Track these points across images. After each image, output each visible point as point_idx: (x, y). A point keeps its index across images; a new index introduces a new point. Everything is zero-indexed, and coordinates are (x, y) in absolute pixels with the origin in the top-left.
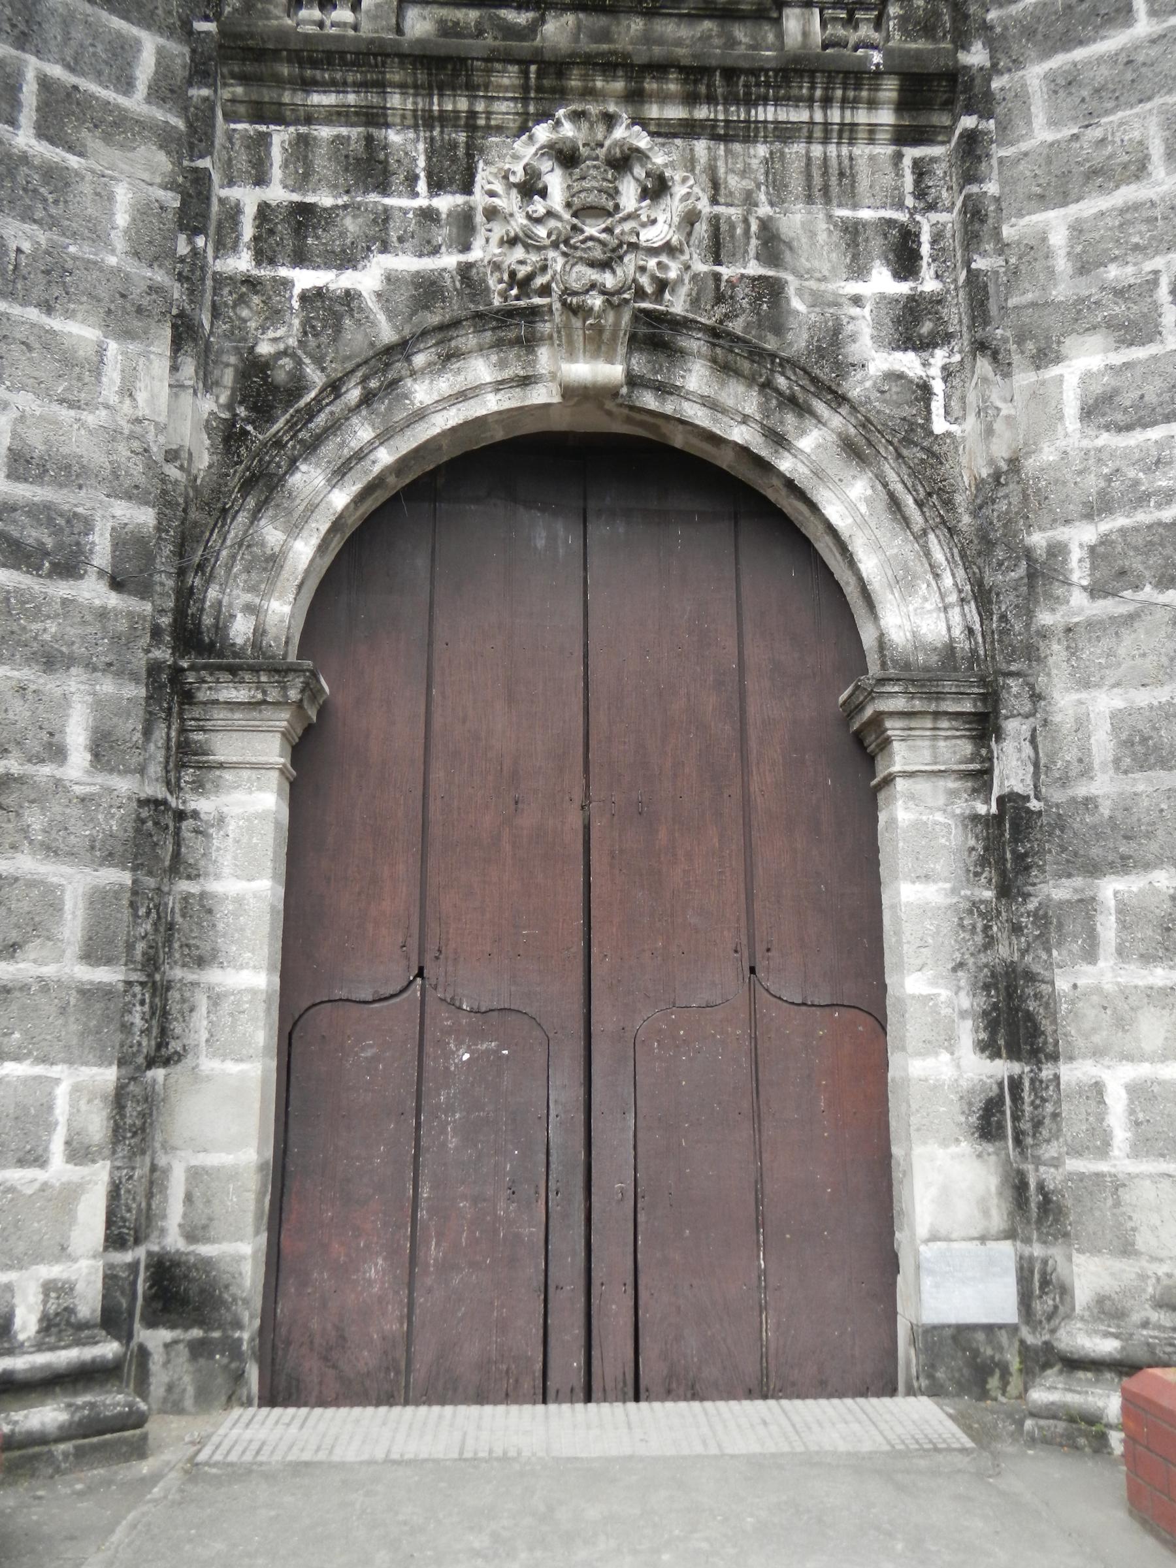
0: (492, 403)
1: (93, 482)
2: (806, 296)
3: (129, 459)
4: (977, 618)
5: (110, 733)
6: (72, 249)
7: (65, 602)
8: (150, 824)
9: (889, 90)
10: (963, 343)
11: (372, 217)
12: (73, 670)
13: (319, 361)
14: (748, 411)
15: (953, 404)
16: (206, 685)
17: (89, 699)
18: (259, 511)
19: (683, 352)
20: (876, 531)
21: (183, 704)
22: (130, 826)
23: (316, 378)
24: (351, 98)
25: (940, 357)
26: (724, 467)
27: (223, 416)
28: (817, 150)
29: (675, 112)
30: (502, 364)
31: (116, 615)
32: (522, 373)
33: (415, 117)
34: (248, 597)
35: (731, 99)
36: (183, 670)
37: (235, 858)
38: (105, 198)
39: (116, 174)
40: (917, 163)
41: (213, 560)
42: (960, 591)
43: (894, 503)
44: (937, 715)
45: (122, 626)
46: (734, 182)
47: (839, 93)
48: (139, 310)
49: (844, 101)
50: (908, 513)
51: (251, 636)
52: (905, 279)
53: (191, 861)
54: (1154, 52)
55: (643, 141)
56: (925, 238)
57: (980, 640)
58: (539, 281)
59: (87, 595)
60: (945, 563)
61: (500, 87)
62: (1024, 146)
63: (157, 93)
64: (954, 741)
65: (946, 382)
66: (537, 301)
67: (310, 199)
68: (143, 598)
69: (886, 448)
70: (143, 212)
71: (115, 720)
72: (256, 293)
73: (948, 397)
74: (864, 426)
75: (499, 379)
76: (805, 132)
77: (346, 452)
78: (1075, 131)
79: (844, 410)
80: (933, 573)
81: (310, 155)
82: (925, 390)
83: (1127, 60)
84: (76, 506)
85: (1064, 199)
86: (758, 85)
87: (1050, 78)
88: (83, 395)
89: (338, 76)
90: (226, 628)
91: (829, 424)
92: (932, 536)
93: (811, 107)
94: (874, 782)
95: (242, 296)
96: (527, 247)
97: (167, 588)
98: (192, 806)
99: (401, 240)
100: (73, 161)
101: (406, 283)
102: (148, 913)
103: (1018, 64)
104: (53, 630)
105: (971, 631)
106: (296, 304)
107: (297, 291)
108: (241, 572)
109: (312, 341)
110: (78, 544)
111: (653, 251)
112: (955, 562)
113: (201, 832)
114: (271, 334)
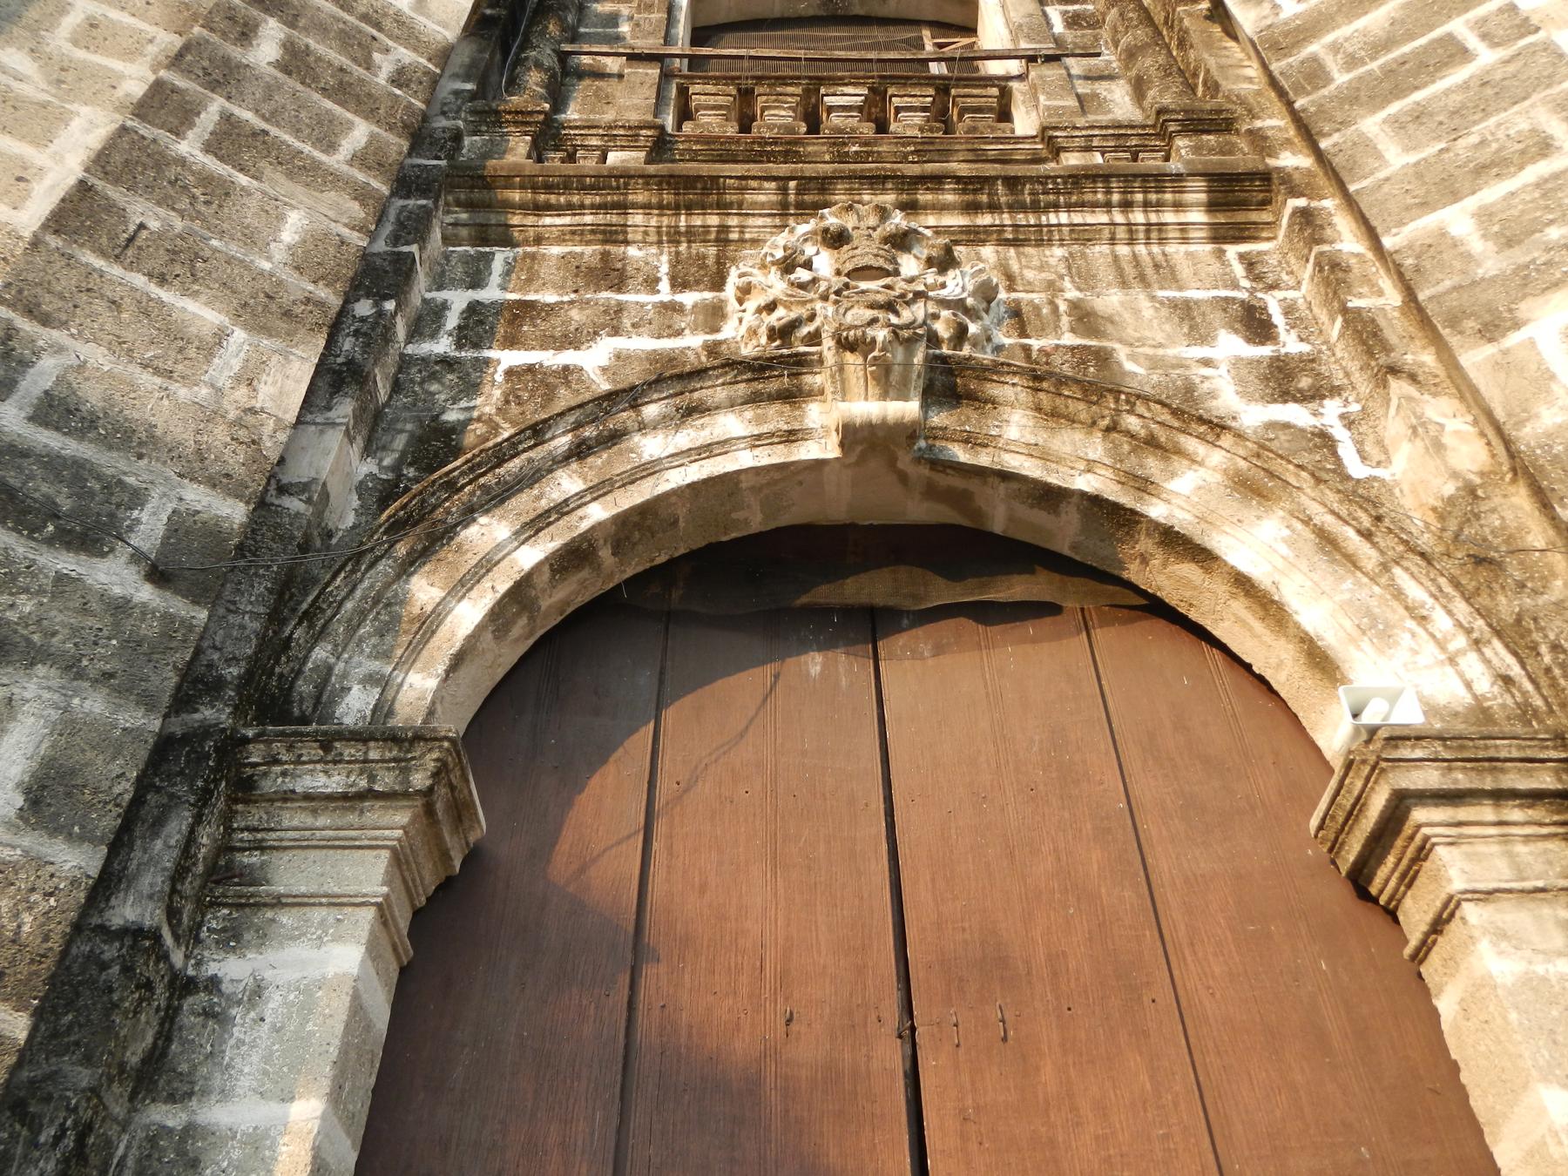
1: (164, 456)
2: (1142, 360)
3: (226, 445)
4: (1510, 660)
5: (73, 772)
6: (214, 243)
7: (61, 578)
8: (116, 969)
9: (1196, 193)
11: (602, 309)
12: (41, 670)
14: (1091, 456)
15: (1367, 449)
16: (277, 769)
17: (55, 715)
18: (412, 564)
19: (993, 402)
20: (1312, 574)
21: (236, 801)
22: (59, 930)
24: (588, 219)
26: (1066, 552)
27: (384, 477)
31: (144, 614)
32: (785, 427)
33: (659, 233)
34: (374, 665)
36: (246, 741)
37: (267, 1059)
39: (293, 202)
41: (329, 612)
42: (1469, 631)
43: (1327, 541)
44: (1499, 796)
45: (150, 629)
47: (1139, 197)
49: (1146, 205)
50: (1351, 549)
51: (368, 713)
52: (1262, 343)
53: (184, 1068)
54: (1511, 68)
57: (1529, 686)
59: (102, 578)
60: (1430, 601)
61: (754, 205)
64: (1541, 845)
65: (1349, 429)
67: (531, 297)
68: (195, 602)
69: (1297, 475)
71: (90, 755)
72: (453, 371)
74: (1258, 456)
75: (756, 432)
76: (1106, 234)
77: (544, 504)
78: (1443, 145)
79: (1227, 440)
80: (1414, 618)
81: (536, 267)
84: (125, 473)
85: (1455, 196)
86: (1045, 193)
88: (180, 367)
89: (575, 199)
90: (333, 703)
91: (1207, 463)
92: (1397, 571)
93: (1109, 212)
94: (1408, 951)
95: (434, 373)
97: (247, 632)
98: (212, 969)
100: (243, 180)
101: (639, 359)
102: (58, 1139)
104: (27, 609)
105: (1507, 681)
106: (499, 377)
107: (501, 369)
108: (370, 635)
109: (514, 409)
110: (112, 515)
112: (1446, 596)
113: (215, 1016)
114: (463, 404)
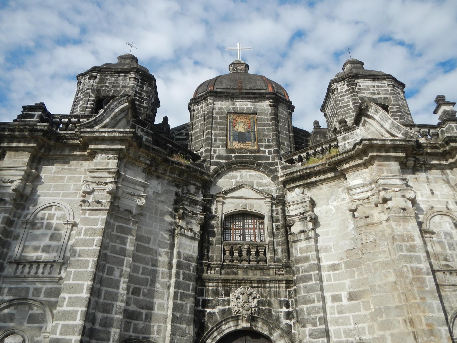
0: (233, 329)
9: (284, 282)
10: (295, 319)
13: (210, 323)
19: (258, 321)
23: (210, 326)
25: (293, 321)
28: (275, 289)
29: (256, 285)
30: (234, 323)
35: (263, 283)
38: (187, 307)
40: (289, 291)
46: (264, 294)
48: (190, 321)
49: (278, 283)
54: (315, 286)
55: (252, 291)
56: (290, 302)
58: (239, 312)
62: (301, 295)
63: (192, 291)
66: (239, 315)
67: (209, 298)
70: (190, 307)
73: (294, 327)
79: (280, 330)
82: (291, 326)
83: (312, 286)
85: (306, 304)
87: (303, 286)
96: (237, 307)
99: (220, 304)
100: (183, 302)
103: (299, 283)
111: (254, 307)
